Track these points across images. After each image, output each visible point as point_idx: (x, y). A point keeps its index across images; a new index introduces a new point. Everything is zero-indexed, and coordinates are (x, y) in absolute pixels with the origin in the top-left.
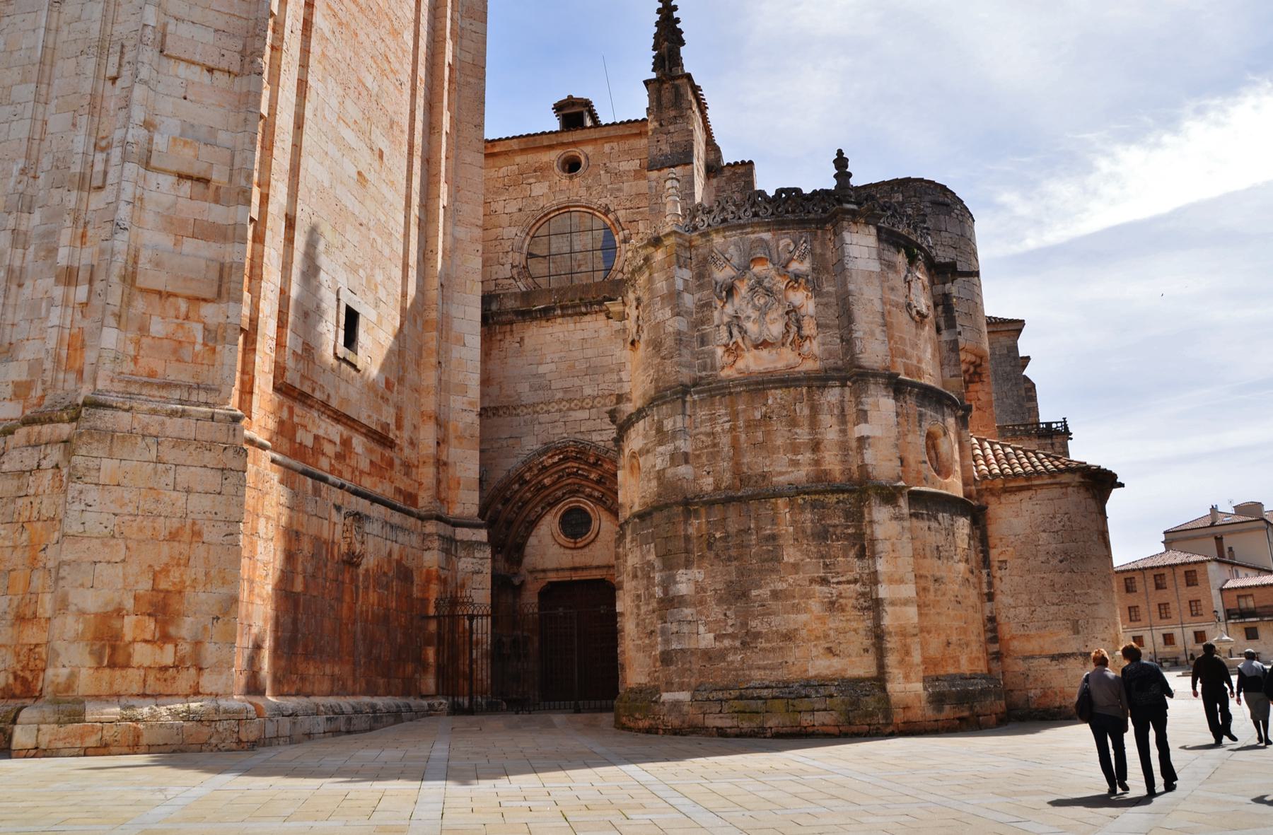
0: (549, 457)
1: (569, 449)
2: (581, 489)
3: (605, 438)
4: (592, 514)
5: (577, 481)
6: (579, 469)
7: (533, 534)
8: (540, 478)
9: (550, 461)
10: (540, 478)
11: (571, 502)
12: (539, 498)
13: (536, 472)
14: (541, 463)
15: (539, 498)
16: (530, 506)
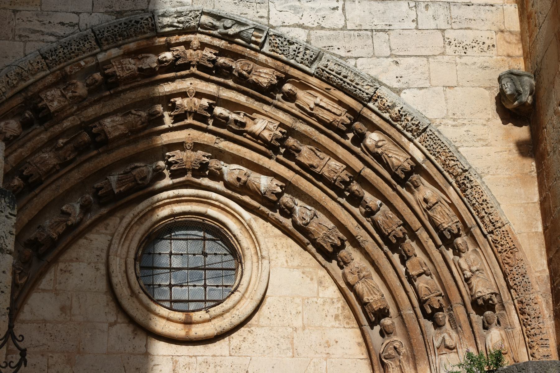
0: (129, 54)
1: (195, 39)
2: (214, 164)
3: (306, 21)
4: (245, 242)
5: (207, 138)
6: (218, 101)
7: (44, 283)
8: (91, 112)
9: (132, 65)
10: (91, 112)
11: (179, 200)
12: (76, 176)
13: (81, 89)
14: (99, 67)
15: (76, 176)
16: (47, 195)
